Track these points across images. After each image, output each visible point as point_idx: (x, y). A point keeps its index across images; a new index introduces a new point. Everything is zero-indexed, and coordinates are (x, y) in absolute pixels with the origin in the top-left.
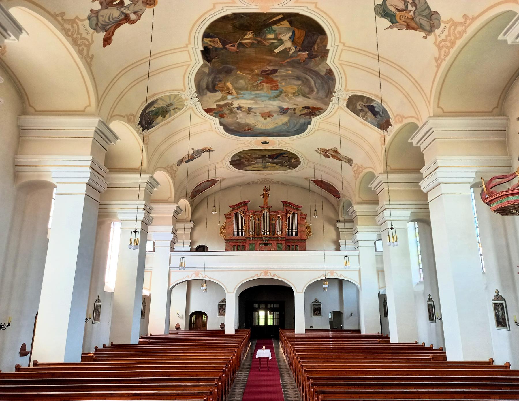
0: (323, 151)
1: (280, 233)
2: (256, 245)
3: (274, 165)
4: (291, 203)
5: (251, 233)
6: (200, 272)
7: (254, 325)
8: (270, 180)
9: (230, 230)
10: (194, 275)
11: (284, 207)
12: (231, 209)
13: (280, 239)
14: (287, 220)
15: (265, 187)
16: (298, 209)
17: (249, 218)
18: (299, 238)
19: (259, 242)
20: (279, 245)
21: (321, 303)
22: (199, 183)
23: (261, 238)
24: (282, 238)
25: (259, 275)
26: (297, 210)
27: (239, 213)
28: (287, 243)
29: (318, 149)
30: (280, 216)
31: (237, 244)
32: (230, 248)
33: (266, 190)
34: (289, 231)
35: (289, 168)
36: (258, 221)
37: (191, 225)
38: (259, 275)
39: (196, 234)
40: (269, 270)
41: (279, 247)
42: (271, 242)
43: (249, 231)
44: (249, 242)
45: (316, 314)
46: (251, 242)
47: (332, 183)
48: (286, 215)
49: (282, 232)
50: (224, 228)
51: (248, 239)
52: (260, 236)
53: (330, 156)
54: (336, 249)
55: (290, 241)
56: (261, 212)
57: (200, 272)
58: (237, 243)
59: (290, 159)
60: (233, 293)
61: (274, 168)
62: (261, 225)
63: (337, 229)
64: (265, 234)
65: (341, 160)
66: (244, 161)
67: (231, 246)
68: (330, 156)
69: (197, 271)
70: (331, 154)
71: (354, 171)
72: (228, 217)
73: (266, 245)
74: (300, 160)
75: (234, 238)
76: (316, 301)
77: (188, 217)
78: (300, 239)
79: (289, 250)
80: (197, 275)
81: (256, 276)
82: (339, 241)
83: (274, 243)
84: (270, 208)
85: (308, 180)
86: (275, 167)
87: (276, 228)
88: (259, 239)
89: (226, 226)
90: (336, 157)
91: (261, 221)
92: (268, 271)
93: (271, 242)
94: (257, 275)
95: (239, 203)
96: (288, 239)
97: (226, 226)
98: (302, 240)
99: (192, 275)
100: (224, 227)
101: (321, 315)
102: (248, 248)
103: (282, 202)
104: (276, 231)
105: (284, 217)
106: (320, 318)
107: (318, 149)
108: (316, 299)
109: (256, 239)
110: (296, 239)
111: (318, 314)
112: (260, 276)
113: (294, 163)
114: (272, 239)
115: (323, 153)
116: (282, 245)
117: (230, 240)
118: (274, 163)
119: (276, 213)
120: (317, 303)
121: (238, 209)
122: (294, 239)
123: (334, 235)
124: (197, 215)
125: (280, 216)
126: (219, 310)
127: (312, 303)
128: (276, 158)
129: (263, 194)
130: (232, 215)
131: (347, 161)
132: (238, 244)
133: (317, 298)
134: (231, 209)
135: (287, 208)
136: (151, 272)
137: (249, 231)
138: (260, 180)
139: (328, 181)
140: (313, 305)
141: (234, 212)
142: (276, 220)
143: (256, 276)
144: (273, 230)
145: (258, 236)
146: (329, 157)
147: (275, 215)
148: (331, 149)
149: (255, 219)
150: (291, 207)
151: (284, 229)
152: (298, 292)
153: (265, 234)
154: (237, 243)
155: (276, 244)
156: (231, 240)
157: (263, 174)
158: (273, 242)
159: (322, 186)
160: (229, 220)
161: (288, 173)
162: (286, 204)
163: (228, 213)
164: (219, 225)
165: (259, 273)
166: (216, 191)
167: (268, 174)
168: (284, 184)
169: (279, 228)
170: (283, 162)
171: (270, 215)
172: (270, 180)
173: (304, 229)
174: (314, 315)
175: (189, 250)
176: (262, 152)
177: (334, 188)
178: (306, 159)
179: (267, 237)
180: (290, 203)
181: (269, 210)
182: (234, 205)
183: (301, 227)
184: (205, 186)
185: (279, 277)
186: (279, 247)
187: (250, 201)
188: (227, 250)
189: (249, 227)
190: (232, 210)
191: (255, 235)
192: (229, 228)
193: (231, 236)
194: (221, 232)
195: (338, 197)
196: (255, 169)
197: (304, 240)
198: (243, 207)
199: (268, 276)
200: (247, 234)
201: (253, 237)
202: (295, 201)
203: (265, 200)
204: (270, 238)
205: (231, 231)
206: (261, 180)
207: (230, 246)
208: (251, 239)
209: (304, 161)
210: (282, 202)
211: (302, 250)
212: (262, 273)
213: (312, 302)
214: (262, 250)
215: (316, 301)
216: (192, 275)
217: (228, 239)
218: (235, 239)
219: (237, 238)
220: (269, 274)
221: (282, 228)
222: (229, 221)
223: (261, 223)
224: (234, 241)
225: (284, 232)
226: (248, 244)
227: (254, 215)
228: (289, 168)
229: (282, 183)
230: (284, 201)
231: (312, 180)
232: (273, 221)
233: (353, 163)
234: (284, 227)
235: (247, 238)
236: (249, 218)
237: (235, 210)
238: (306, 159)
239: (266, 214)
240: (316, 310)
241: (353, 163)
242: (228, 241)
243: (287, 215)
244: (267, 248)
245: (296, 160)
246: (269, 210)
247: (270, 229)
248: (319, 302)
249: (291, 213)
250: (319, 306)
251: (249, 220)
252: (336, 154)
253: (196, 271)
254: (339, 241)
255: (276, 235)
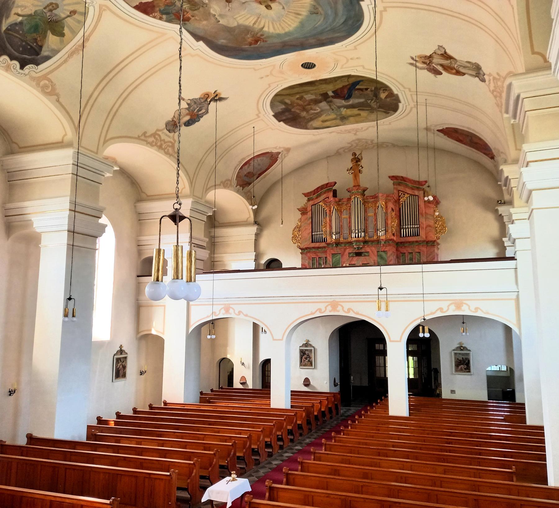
0: (424, 63)
1: (381, 234)
2: (342, 256)
3: (355, 111)
4: (406, 178)
5: (334, 237)
6: (231, 306)
7: (378, 375)
8: (369, 142)
9: (307, 233)
10: (223, 311)
11: (395, 186)
12: (306, 198)
13: (383, 243)
14: (400, 209)
15: (354, 154)
16: (420, 188)
17: (330, 211)
18: (422, 239)
19: (348, 251)
20: (381, 253)
21: (470, 351)
22: (240, 162)
23: (351, 243)
24: (387, 241)
25: (323, 309)
26: (418, 189)
27: (321, 204)
28: (400, 249)
29: (412, 58)
30: (381, 203)
31: (317, 255)
32: (307, 262)
33: (357, 160)
34: (416, 226)
35: (385, 112)
36: (345, 216)
37: (254, 229)
38: (323, 309)
39: (264, 243)
40: (339, 300)
41: (382, 258)
42: (368, 249)
43: (331, 234)
44: (331, 250)
45: (461, 370)
46: (334, 251)
47: (473, 130)
48: (397, 201)
49: (386, 231)
50: (299, 231)
51: (330, 246)
52: (349, 239)
53: (440, 69)
54: (498, 254)
55: (406, 245)
56: (349, 199)
57: (231, 306)
58: (318, 254)
59: (376, 95)
60: (282, 340)
61: (357, 118)
62: (350, 222)
63: (500, 218)
64: (358, 237)
65: (464, 74)
66: (298, 111)
67: (309, 258)
68: (440, 69)
69: (228, 304)
70: (442, 65)
71: (493, 92)
72: (303, 211)
73: (358, 254)
74: (395, 92)
75: (313, 245)
76: (461, 348)
77: (250, 217)
78: (424, 241)
79: (404, 264)
80: (227, 310)
81: (318, 312)
82: (504, 239)
83: (373, 252)
84: (364, 191)
85: (433, 131)
86: (359, 115)
87: (376, 225)
88: (347, 245)
89: (301, 226)
90: (452, 68)
91: (350, 214)
92: (337, 302)
93: (368, 249)
94: (320, 310)
95: (318, 188)
96: (401, 243)
97: (301, 226)
98: (427, 242)
99: (220, 311)
100: (298, 228)
101: (469, 372)
102: (330, 261)
103: (389, 177)
104: (377, 230)
105: (391, 205)
106: (469, 377)
107: (412, 58)
108: (460, 343)
109: (343, 245)
110: (417, 242)
111: (465, 369)
112: (325, 311)
113: (388, 100)
114: (370, 243)
115: (425, 66)
116: (387, 254)
117: (306, 248)
118: (352, 106)
119: (375, 197)
120: (462, 350)
121: (317, 198)
122: (413, 242)
123: (494, 229)
124: (264, 214)
125: (381, 203)
126: (301, 358)
127: (454, 350)
128: (349, 97)
129: (351, 168)
130: (309, 209)
131: (474, 73)
132: (320, 255)
133: (463, 342)
134: (306, 198)
135: (401, 188)
136: (164, 306)
137: (330, 232)
138: (352, 145)
139: (463, 127)
140: (455, 354)
141: (311, 203)
142: (375, 210)
143: (318, 312)
144: (371, 230)
145: (345, 241)
146: (440, 74)
147: (373, 202)
148: (435, 53)
149: (339, 212)
150: (407, 186)
151: (389, 226)
152: (399, 340)
153: (358, 237)
154: (318, 254)
155: (376, 253)
156: (308, 250)
157: (349, 132)
158: (371, 250)
159: (461, 138)
160: (305, 216)
161: (390, 124)
162: (398, 180)
163: (303, 206)
164: (281, 226)
165: (322, 306)
166: (284, 173)
167: (357, 131)
168: (398, 146)
169: (380, 225)
170: (366, 101)
171: (365, 202)
172: (369, 142)
173: (431, 222)
174: (456, 371)
175: (252, 266)
176: (314, 88)
177: (480, 139)
178: (405, 88)
179: (357, 241)
180: (403, 179)
181: (363, 195)
182: (311, 192)
183: (426, 218)
184: (259, 165)
185: (357, 314)
186: (382, 258)
187: (335, 183)
188: (304, 268)
189: (330, 226)
190: (309, 200)
191: (342, 240)
192: (306, 229)
193: (308, 243)
194: (294, 237)
195: (492, 157)
196: (328, 124)
197: (431, 241)
198: (325, 193)
199: (339, 311)
200: (328, 238)
201: (338, 243)
202: (412, 174)
203: (356, 176)
204: (365, 242)
205: (308, 234)
206: (355, 145)
207: (307, 258)
208: (334, 245)
209: (403, 92)
210: (389, 177)
211: (429, 259)
212: (327, 306)
213: (454, 348)
214: (326, 266)
215: (461, 348)
216: (220, 311)
217: (304, 247)
218: (314, 248)
219: (317, 245)
220: (340, 308)
221: (386, 224)
222: (306, 219)
223: (350, 218)
224: (314, 250)
225: (390, 231)
226: (329, 255)
227: (339, 205)
228: (388, 113)
229: (394, 146)
230: (393, 176)
231: (438, 130)
232: (371, 214)
233: (484, 75)
234: (389, 222)
235: (328, 244)
236: (330, 211)
237: (312, 200)
238: (405, 88)
239: (357, 200)
240: (460, 362)
241: (484, 75)
242: (304, 251)
243: (400, 199)
244: (361, 259)
245: (386, 93)
246: (363, 195)
247: (366, 227)
248: (465, 348)
249: (406, 196)
250: (466, 357)
251: (330, 215)
252: (449, 61)
253: (225, 304)
254: (504, 239)
255: (375, 238)
